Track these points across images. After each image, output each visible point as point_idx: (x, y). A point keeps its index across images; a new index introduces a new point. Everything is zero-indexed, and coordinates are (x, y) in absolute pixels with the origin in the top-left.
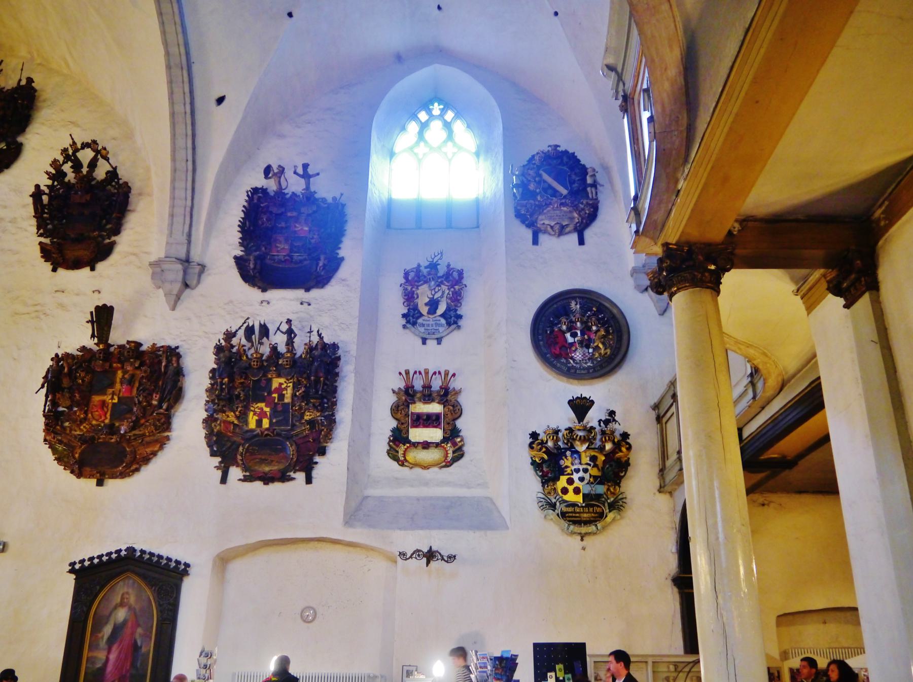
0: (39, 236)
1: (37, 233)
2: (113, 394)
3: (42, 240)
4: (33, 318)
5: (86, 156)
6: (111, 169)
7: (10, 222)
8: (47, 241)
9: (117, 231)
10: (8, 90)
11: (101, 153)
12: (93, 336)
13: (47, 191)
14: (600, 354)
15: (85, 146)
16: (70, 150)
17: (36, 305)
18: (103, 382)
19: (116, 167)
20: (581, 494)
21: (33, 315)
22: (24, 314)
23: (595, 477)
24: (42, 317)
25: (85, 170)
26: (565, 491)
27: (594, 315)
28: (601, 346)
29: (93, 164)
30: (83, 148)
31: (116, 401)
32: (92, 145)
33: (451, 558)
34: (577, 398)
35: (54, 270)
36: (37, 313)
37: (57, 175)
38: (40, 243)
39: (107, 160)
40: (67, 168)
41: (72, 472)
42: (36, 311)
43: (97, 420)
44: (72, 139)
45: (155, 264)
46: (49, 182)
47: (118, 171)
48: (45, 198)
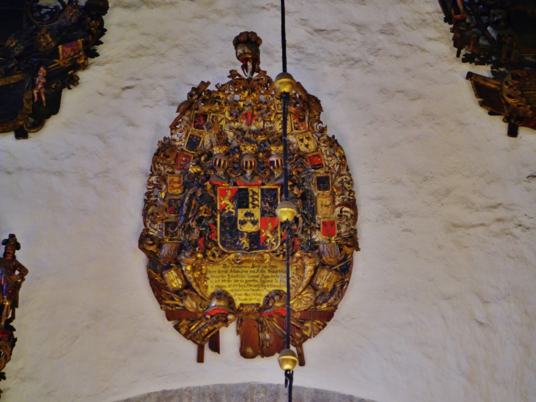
0: (464, 61)
1: (458, 55)
3: (467, 67)
4: (497, 235)
7: (382, 32)
8: (484, 71)
17: (495, 207)
21: (496, 227)
22: (473, 226)
24: (517, 231)
35: (513, 132)
36: (501, 225)
42: (499, 220)
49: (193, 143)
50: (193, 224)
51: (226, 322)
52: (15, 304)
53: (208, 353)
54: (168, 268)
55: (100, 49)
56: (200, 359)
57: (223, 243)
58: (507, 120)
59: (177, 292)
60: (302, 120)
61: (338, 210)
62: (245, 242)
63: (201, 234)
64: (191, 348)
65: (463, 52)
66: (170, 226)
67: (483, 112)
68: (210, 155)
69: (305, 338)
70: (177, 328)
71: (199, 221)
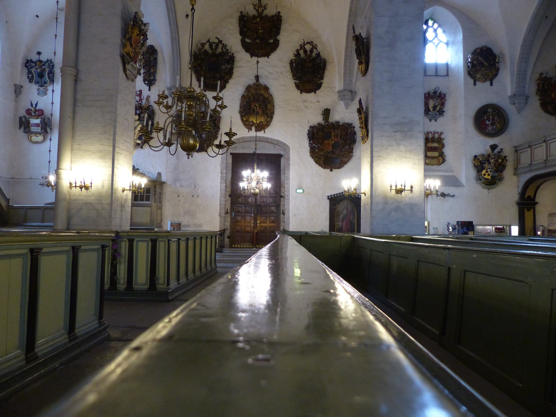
2: (332, 140)
3: (295, 81)
4: (297, 112)
5: (308, 47)
6: (318, 53)
8: (297, 82)
9: (322, 78)
10: (270, 16)
11: (314, 47)
12: (323, 119)
13: (295, 61)
14: (498, 128)
15: (308, 43)
16: (303, 45)
18: (328, 136)
19: (320, 52)
20: (490, 176)
23: (495, 170)
25: (308, 53)
26: (485, 175)
27: (496, 114)
28: (498, 125)
29: (311, 51)
30: (307, 44)
31: (333, 143)
32: (311, 43)
33: (453, 196)
34: (493, 145)
35: (301, 93)
37: (297, 54)
38: (295, 83)
39: (316, 49)
40: (301, 52)
41: (322, 167)
42: (298, 109)
43: (327, 149)
44: (304, 41)
45: (339, 92)
46: (295, 58)
47: (320, 54)
48: (294, 64)
49: (248, 95)
50: (247, 109)
51: (253, 126)
52: (220, 123)
53: (250, 131)
54: (244, 117)
55: (233, 76)
56: (249, 132)
57: (253, 113)
58: (300, 91)
59: (245, 121)
60: (266, 91)
61: (271, 107)
62: (256, 113)
63: (249, 111)
64: (247, 130)
65: (294, 78)
66: (244, 110)
67: (297, 89)
68: (250, 98)
69: (265, 129)
70: (245, 127)
71: (249, 109)
